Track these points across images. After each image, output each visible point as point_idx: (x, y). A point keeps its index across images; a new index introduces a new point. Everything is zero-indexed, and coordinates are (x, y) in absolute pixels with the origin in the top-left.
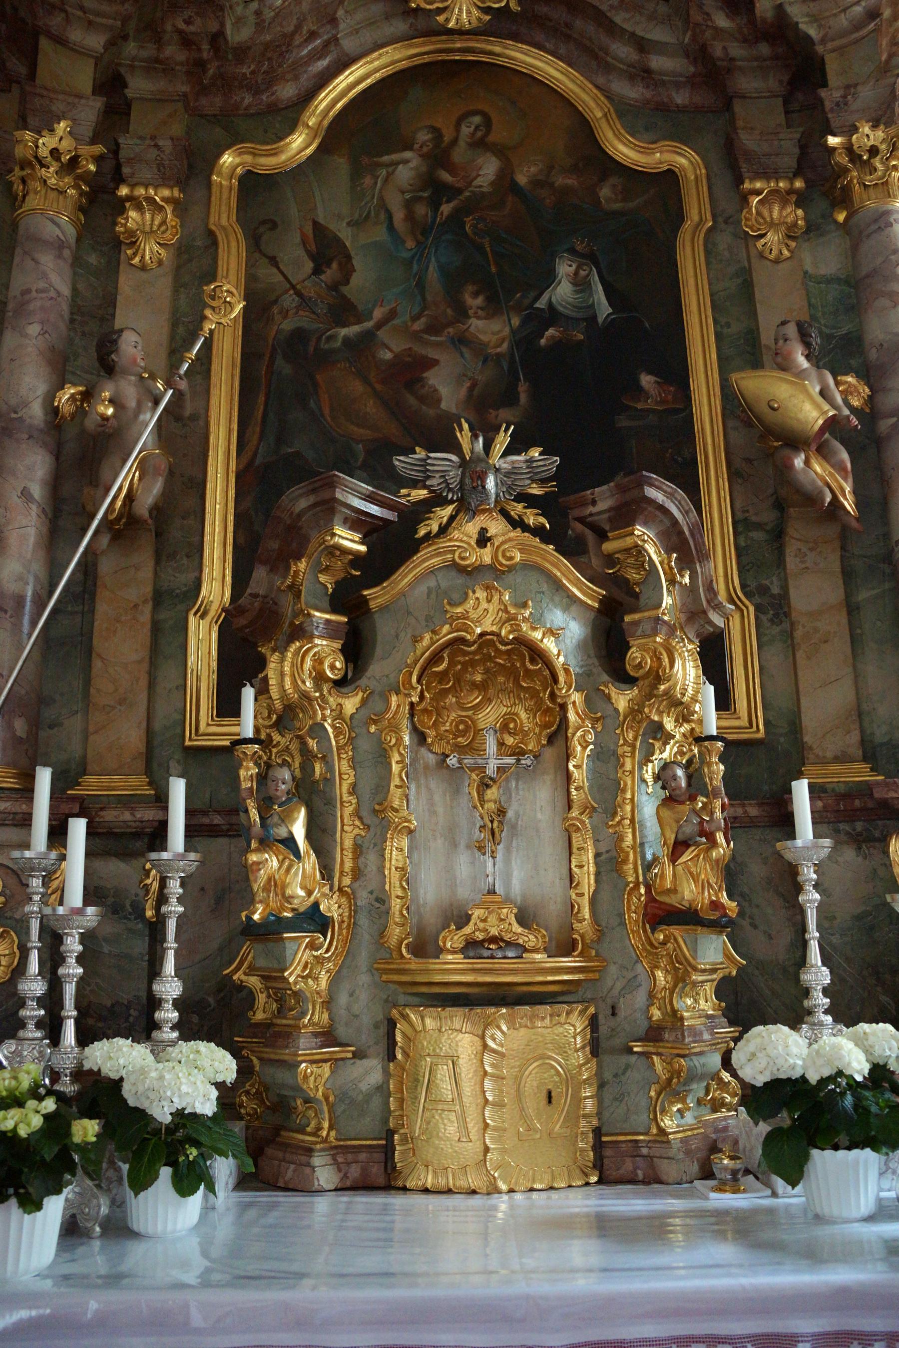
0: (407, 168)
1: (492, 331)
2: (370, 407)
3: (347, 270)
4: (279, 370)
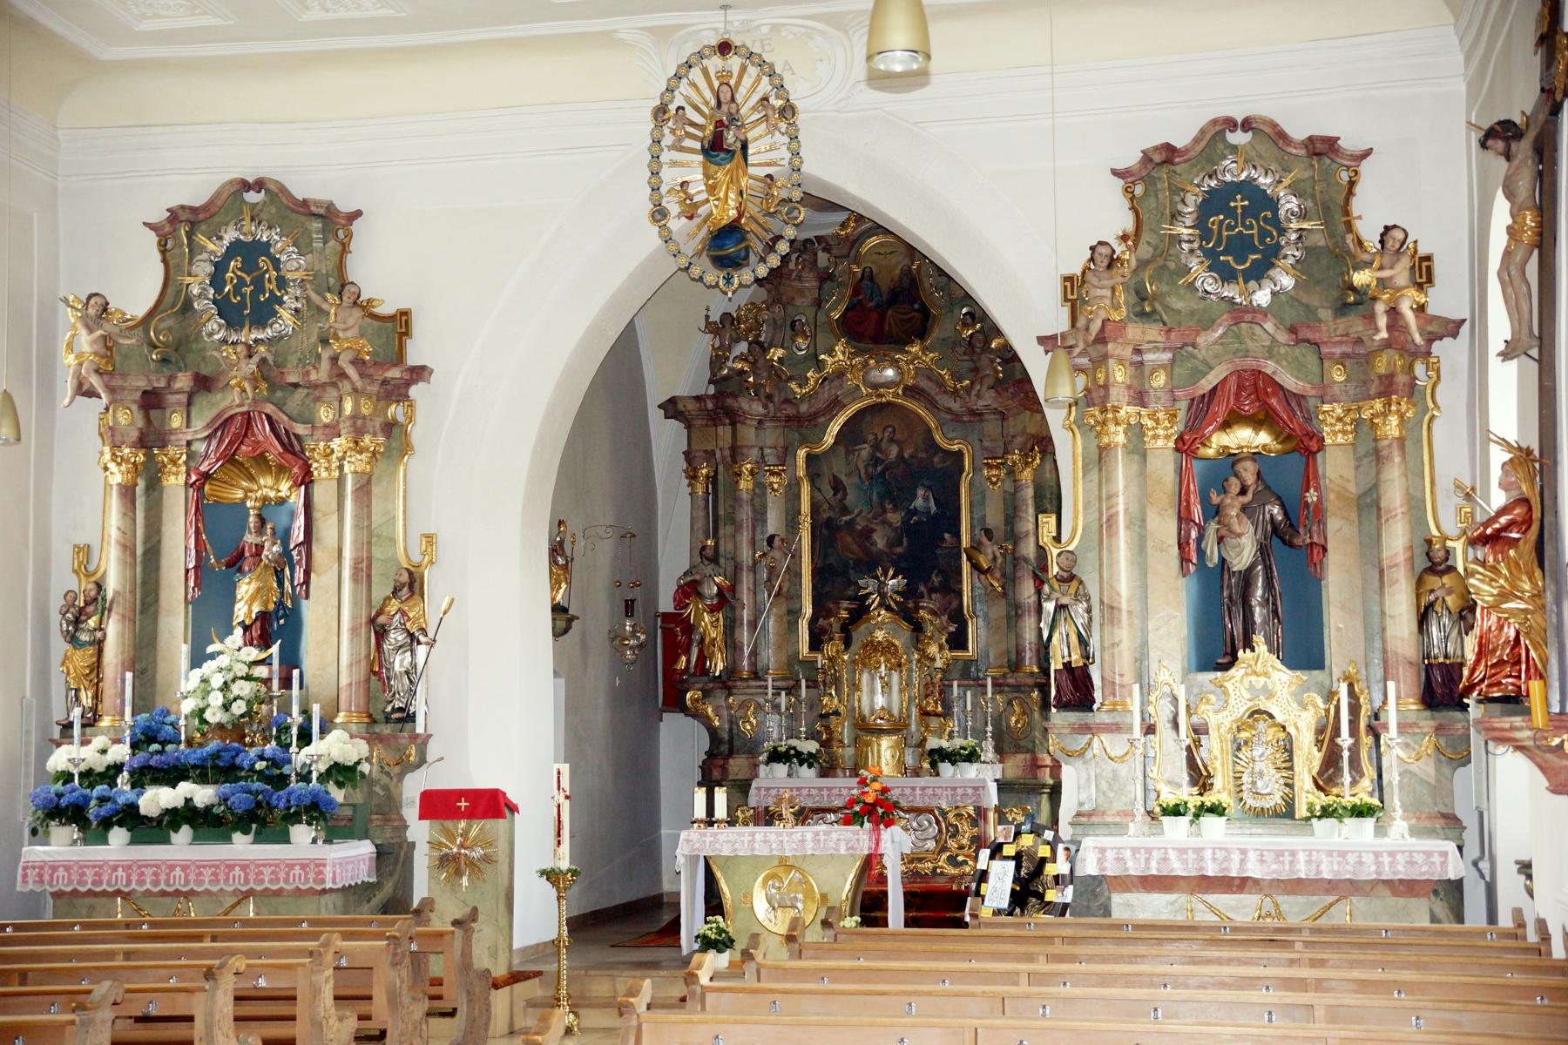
0: (865, 451)
1: (895, 518)
2: (854, 547)
3: (845, 494)
4: (825, 532)
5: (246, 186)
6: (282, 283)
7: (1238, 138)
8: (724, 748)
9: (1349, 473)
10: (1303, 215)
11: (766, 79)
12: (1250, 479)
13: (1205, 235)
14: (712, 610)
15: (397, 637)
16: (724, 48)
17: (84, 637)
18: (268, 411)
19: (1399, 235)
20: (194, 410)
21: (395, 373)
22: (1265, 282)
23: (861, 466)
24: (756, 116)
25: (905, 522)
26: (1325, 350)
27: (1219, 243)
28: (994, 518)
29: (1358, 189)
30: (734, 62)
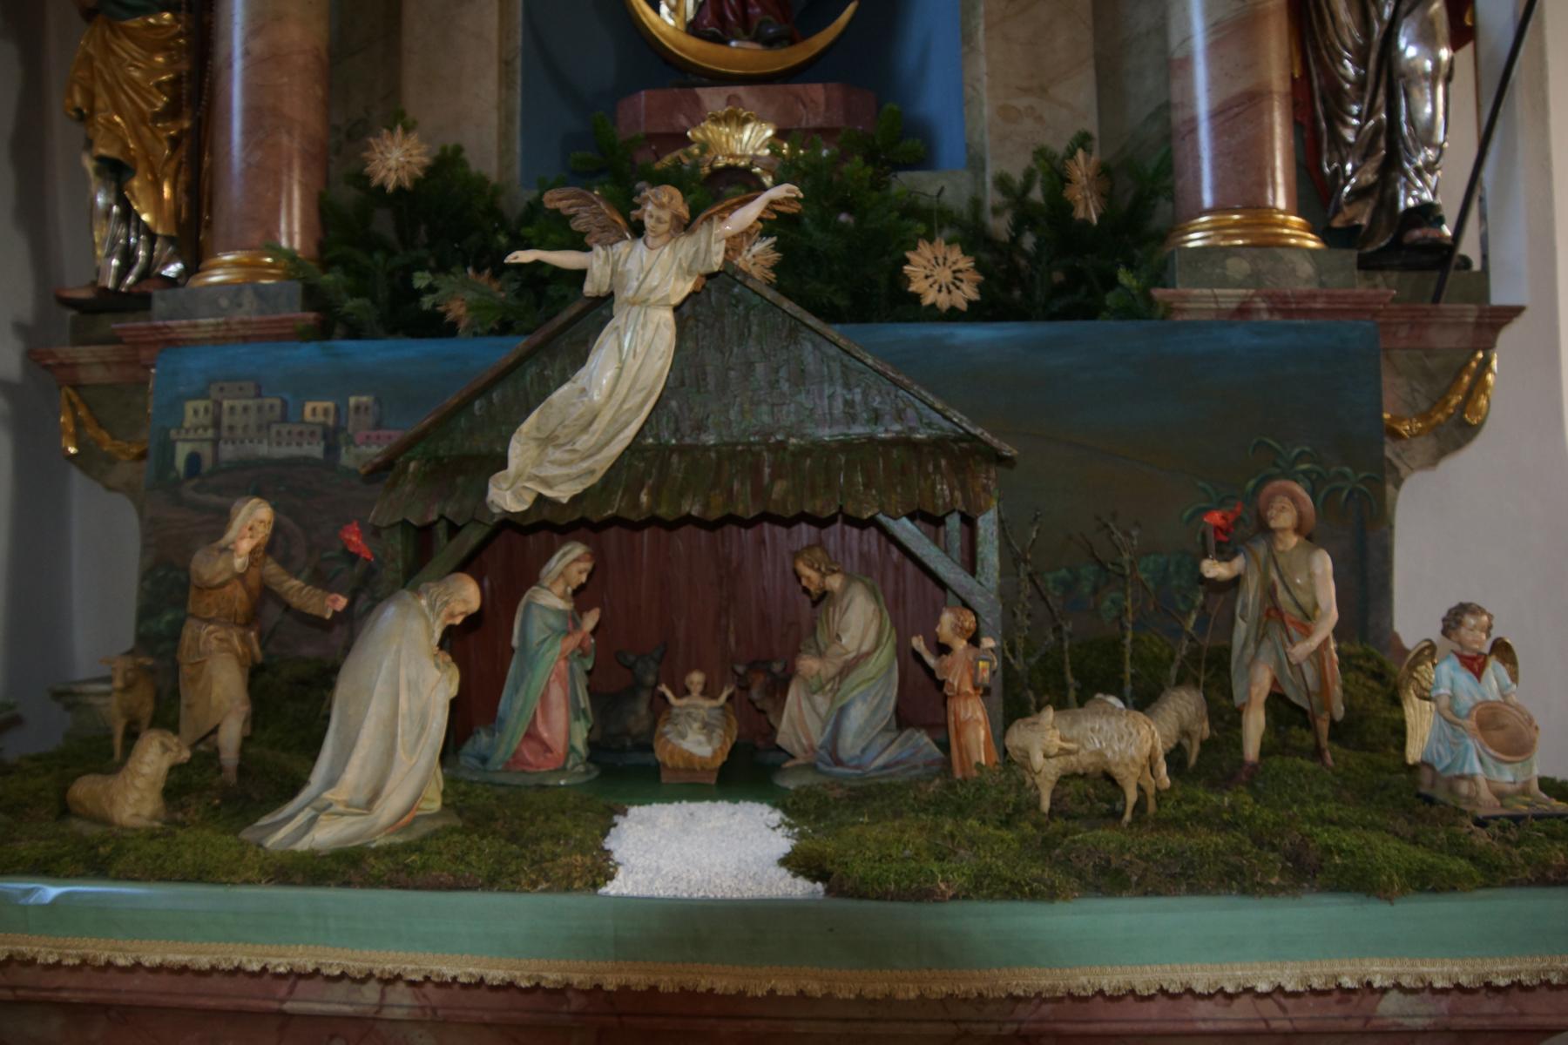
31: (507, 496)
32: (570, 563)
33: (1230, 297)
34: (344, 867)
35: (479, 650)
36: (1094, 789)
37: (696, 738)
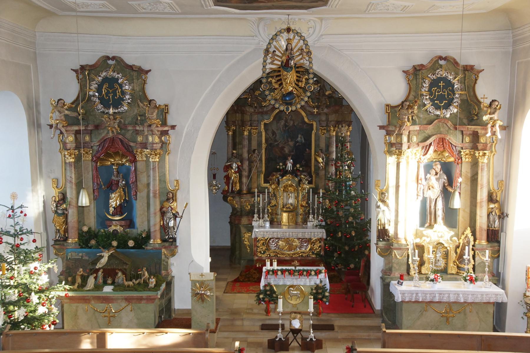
0: (283, 123)
1: (291, 143)
3: (276, 136)
5: (108, 58)
6: (123, 93)
7: (442, 62)
8: (239, 214)
9: (469, 170)
10: (461, 90)
11: (302, 42)
12: (438, 171)
13: (431, 94)
14: (236, 172)
15: (170, 215)
16: (288, 30)
17: (60, 212)
18: (120, 137)
19: (497, 103)
20: (93, 135)
21: (166, 129)
22: (448, 110)
23: (281, 127)
24: (298, 53)
25: (295, 145)
26: (464, 133)
27: (435, 97)
28: (323, 145)
29: (478, 82)
30: (291, 35)
31: (97, 267)
32: (102, 270)
33: (151, 248)
34: (89, 290)
35: (96, 278)
36: (129, 286)
37: (110, 281)
